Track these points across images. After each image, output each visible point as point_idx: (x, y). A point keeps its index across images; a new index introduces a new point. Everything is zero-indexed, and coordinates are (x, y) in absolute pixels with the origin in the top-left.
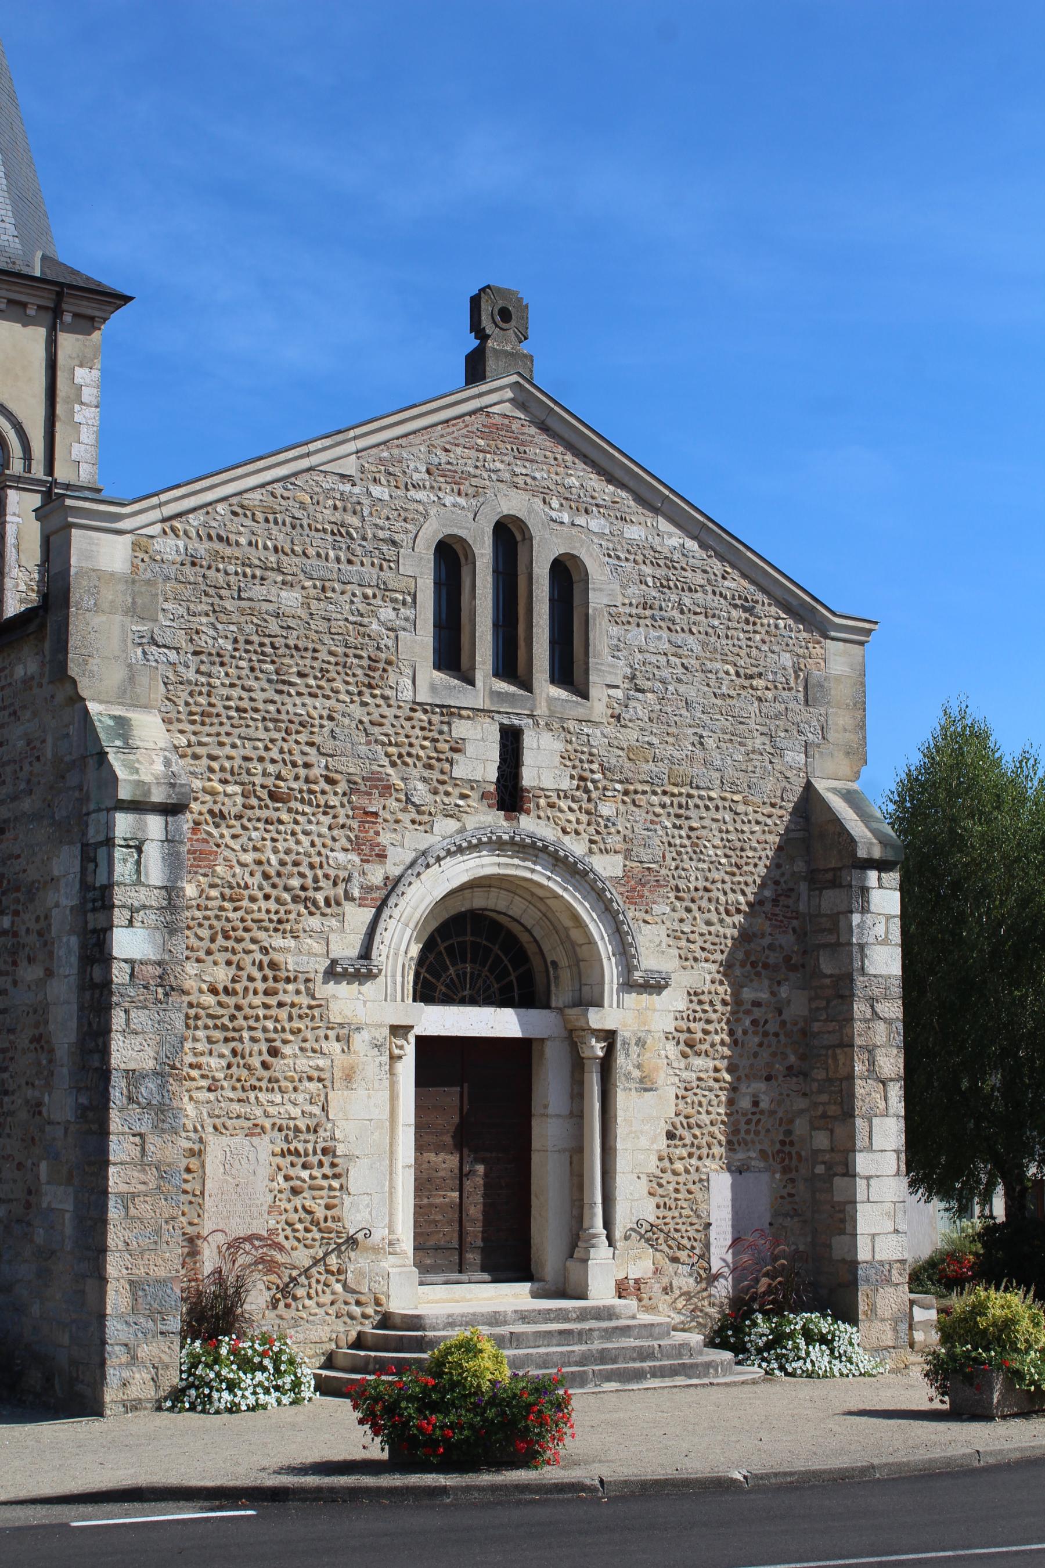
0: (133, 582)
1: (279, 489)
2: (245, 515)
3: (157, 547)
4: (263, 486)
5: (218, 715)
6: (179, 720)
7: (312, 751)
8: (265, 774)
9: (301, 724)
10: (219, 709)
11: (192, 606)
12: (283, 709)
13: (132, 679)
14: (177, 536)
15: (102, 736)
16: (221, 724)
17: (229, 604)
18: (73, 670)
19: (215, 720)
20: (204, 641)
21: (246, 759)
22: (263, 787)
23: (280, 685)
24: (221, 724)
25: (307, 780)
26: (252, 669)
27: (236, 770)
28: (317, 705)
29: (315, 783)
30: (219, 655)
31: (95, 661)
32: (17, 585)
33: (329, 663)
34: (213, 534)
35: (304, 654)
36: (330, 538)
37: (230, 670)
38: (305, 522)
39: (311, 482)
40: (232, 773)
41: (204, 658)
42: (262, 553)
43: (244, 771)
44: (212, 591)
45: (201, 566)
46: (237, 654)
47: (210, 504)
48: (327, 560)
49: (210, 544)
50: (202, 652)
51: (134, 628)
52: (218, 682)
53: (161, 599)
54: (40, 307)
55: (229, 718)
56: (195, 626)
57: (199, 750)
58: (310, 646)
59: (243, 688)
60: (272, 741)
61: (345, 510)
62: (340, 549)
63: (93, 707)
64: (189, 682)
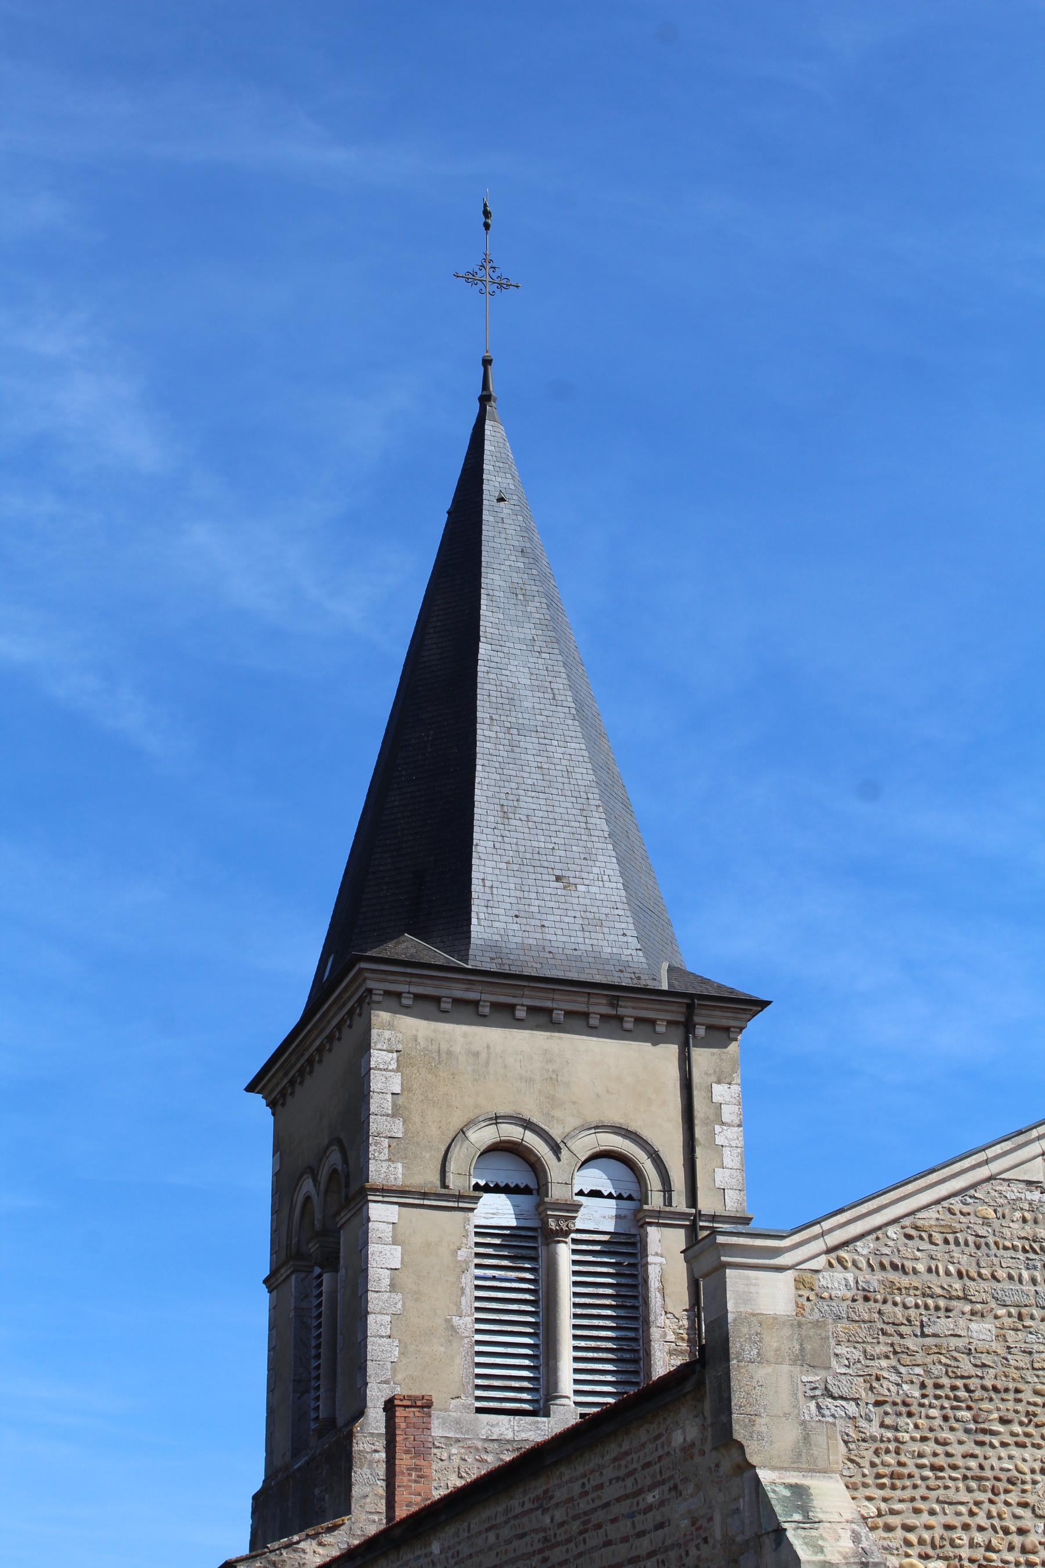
0: (800, 1325)
1: (956, 1204)
2: (921, 1238)
3: (823, 1282)
4: (938, 1202)
5: (910, 1476)
6: (865, 1485)
7: (1026, 1513)
8: (972, 1545)
9: (1010, 1481)
10: (911, 1468)
11: (869, 1348)
12: (987, 1464)
13: (806, 1438)
14: (845, 1268)
15: (778, 1509)
16: (915, 1487)
17: (911, 1343)
18: (739, 1433)
19: (908, 1483)
20: (887, 1389)
21: (948, 1527)
22: (971, 1561)
23: (981, 1433)
24: (915, 1487)
25: (1024, 1550)
26: (946, 1418)
27: (937, 1542)
28: (1027, 1456)
29: (1034, 1553)
30: (905, 1404)
31: (763, 1421)
32: (665, 1335)
33: (1035, 1404)
34: (886, 1262)
35: (1005, 1396)
36: (1021, 1256)
37: (920, 1422)
38: (991, 1240)
39: (993, 1193)
40: (933, 1546)
41: (888, 1408)
42: (944, 1281)
43: (946, 1543)
44: (890, 1329)
45: (876, 1301)
46: (926, 1401)
47: (879, 1228)
48: (1020, 1282)
49: (883, 1274)
50: (885, 1402)
51: (805, 1379)
52: (906, 1437)
53: (833, 1342)
54: (670, 1023)
55: (924, 1479)
56: (875, 1371)
57: (892, 1520)
58: (1011, 1386)
59: (937, 1442)
60: (977, 1503)
61: (1036, 1222)
62: (1035, 1268)
63: (765, 1476)
64: (873, 1439)
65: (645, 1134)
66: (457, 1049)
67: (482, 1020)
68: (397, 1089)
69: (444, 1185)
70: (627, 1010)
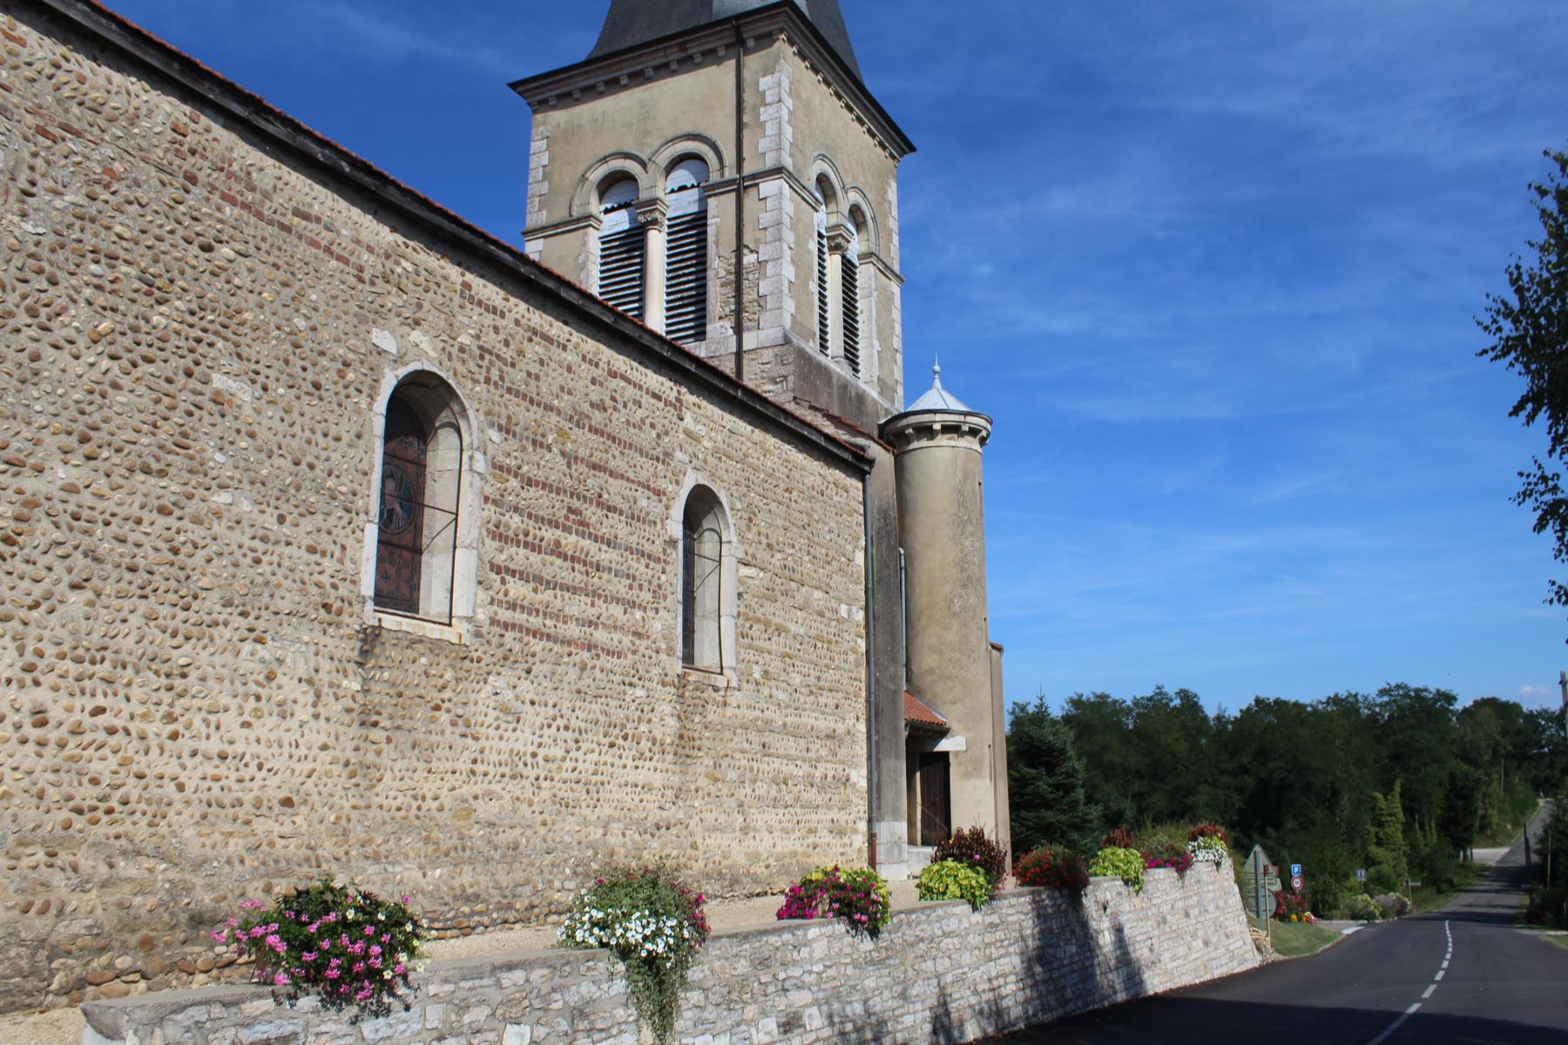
65: (708, 133)
66: (584, 121)
67: (602, 95)
70: (694, 49)
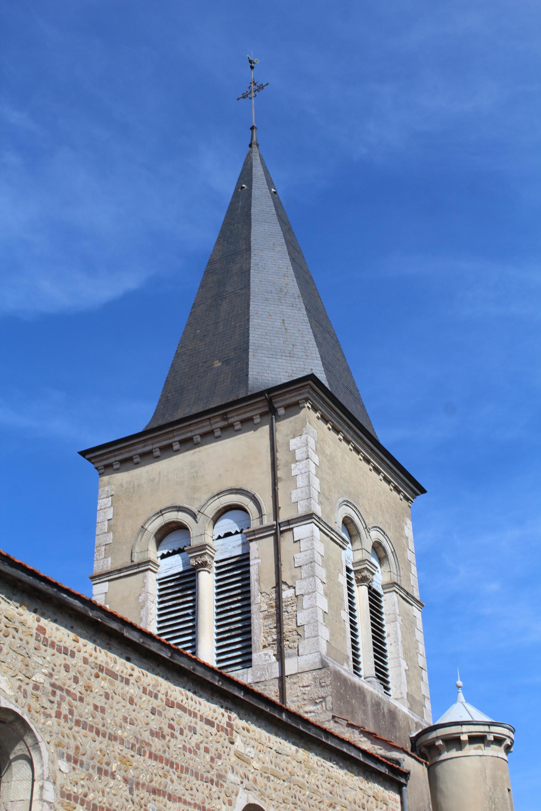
32: (260, 607)
54: (262, 415)
65: (248, 488)
67: (157, 458)
68: (110, 517)
69: (132, 561)
70: (234, 419)
